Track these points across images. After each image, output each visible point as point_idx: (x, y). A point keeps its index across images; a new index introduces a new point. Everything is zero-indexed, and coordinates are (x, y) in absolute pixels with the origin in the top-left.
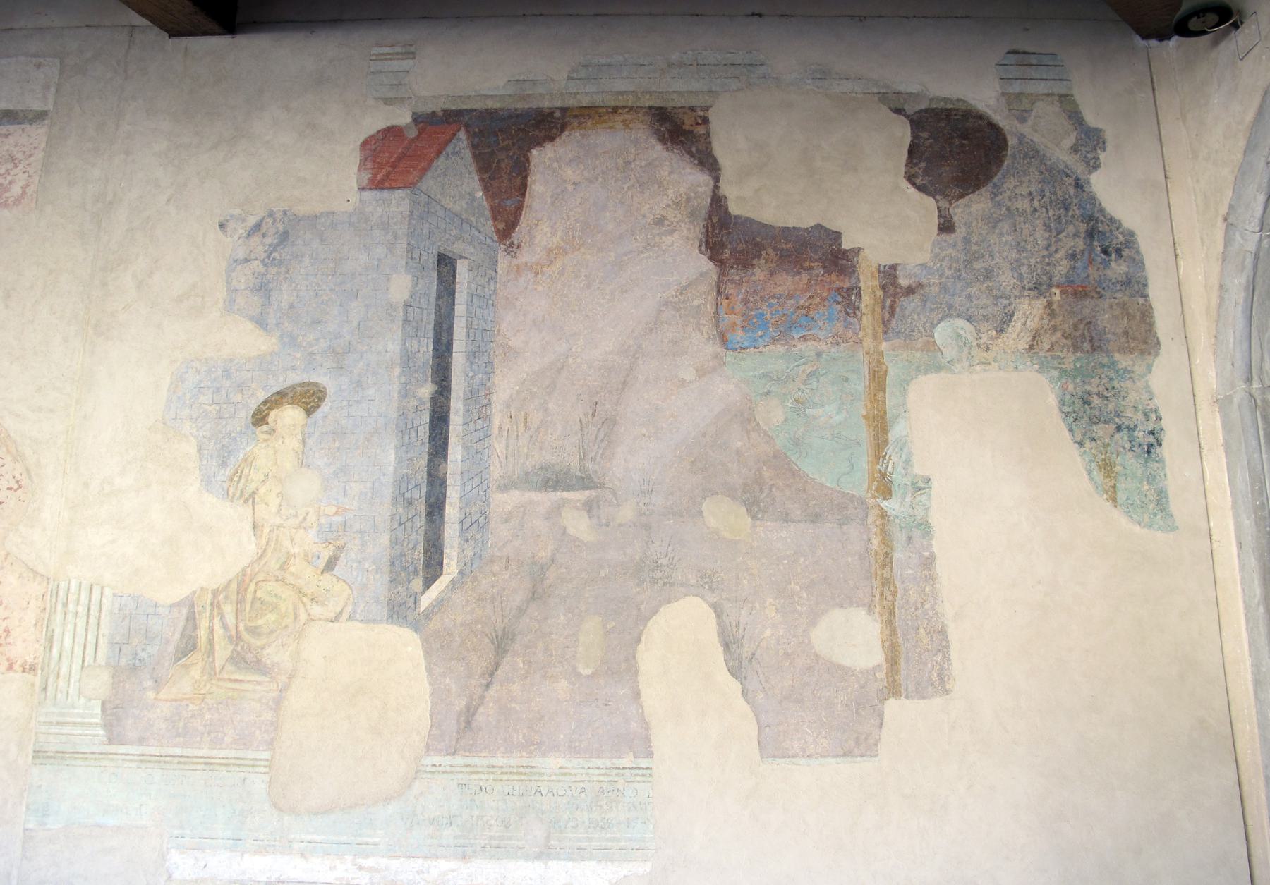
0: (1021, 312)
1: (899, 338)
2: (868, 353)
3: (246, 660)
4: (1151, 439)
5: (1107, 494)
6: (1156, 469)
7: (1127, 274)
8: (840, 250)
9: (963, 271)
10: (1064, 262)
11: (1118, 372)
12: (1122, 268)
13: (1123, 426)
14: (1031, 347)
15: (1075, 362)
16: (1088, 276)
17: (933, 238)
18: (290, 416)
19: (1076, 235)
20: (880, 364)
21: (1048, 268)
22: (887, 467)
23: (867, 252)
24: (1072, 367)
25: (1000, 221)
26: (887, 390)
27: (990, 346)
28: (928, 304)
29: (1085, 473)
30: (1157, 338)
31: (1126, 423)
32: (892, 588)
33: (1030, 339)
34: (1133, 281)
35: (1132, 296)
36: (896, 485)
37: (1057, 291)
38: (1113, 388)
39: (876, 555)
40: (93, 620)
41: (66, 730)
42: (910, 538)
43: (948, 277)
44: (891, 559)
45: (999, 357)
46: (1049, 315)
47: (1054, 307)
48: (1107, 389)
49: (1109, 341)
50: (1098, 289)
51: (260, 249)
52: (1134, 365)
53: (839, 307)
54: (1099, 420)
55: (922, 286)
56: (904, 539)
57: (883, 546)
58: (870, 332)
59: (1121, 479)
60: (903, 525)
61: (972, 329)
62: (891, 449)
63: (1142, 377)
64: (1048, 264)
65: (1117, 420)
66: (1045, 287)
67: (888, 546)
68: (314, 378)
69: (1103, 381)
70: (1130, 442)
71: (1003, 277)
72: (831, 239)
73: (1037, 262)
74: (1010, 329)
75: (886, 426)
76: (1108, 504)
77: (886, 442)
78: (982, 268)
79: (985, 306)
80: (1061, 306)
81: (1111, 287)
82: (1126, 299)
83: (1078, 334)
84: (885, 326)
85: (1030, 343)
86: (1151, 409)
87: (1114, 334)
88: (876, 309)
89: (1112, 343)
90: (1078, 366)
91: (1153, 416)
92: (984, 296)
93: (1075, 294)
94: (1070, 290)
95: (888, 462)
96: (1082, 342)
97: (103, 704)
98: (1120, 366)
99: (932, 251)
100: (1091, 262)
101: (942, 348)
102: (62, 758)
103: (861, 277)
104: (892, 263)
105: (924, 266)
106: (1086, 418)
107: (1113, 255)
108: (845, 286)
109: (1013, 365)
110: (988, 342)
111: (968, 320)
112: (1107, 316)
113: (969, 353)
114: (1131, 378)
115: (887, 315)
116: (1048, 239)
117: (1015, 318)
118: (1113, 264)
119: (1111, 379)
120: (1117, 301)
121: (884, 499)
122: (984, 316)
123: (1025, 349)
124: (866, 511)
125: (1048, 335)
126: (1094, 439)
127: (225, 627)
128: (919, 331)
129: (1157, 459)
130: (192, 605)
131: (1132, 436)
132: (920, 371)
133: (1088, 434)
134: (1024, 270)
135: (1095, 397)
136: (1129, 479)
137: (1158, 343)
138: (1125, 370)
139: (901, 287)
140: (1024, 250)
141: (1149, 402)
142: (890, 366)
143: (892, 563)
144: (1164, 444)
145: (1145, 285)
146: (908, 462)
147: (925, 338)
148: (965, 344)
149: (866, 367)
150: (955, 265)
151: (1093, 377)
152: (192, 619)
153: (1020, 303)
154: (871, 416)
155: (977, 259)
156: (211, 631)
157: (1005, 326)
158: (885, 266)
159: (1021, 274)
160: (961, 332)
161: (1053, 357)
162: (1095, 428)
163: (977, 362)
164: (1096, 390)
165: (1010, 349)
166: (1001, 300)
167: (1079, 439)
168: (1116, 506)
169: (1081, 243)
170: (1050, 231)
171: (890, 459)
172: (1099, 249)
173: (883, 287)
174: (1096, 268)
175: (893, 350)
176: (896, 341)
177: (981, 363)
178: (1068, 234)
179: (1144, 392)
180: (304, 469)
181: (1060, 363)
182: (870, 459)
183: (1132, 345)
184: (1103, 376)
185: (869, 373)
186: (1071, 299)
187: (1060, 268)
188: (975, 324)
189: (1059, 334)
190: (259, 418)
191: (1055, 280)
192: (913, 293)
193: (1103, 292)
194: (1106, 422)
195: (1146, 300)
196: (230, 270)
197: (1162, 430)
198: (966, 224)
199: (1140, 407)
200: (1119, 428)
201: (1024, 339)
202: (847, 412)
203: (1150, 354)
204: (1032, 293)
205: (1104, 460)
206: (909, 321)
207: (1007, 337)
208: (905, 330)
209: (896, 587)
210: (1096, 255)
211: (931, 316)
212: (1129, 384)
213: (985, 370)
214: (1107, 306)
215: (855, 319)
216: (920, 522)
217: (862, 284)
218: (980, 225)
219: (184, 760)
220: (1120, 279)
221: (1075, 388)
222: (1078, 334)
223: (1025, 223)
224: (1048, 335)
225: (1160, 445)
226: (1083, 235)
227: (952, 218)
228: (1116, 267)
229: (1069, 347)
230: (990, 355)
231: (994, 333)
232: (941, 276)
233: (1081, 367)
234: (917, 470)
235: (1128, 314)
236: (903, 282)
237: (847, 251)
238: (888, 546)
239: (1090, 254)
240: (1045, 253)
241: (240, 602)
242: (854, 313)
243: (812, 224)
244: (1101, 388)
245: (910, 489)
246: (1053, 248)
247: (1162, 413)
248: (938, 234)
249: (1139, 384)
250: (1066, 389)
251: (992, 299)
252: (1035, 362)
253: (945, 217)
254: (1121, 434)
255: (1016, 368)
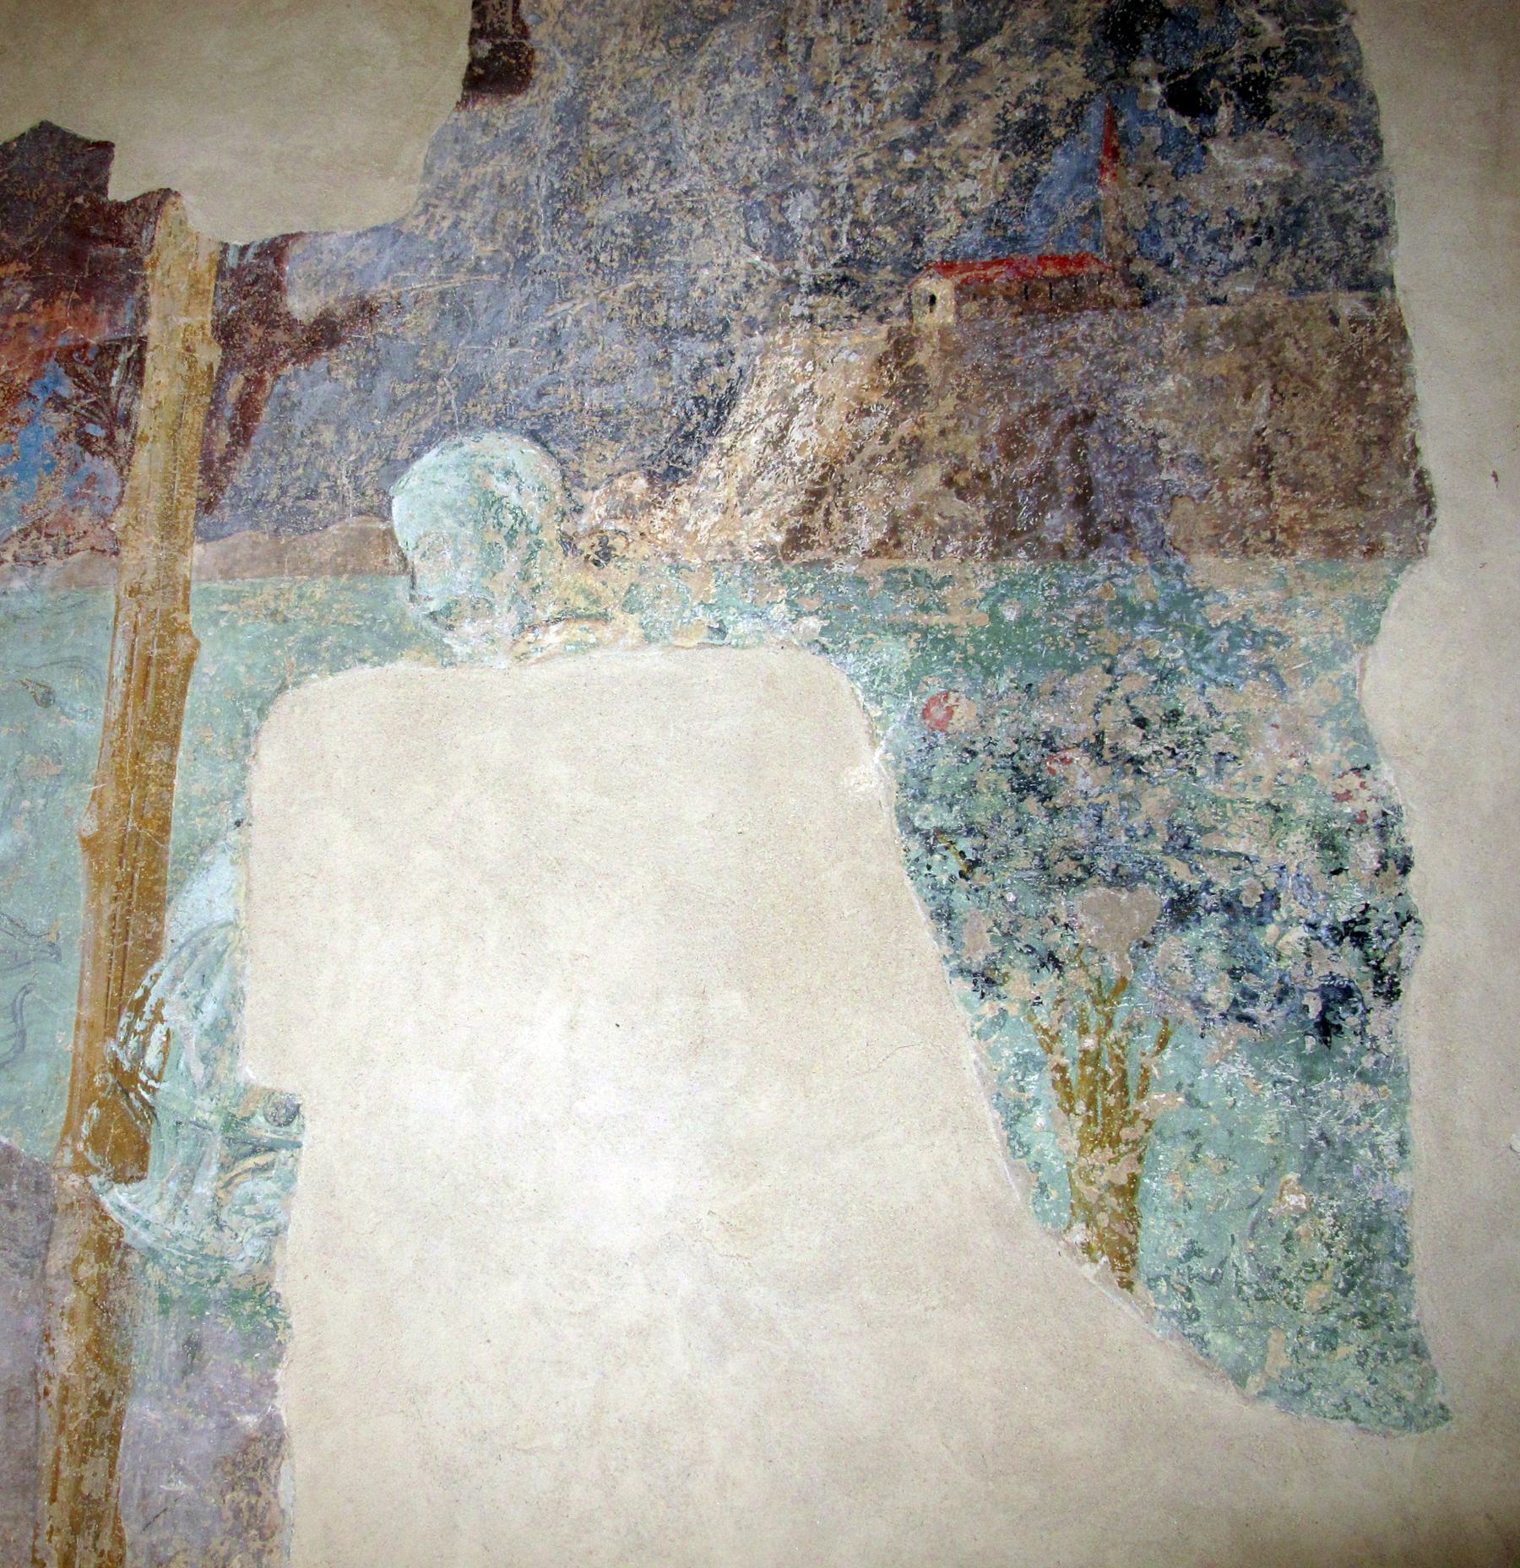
0: (767, 390)
1: (256, 526)
2: (134, 592)
4: (1347, 964)
5: (1090, 1222)
6: (1355, 1109)
7: (1285, 191)
8: (97, 208)
9: (541, 237)
10: (989, 160)
11: (1202, 640)
12: (1266, 162)
13: (1207, 900)
14: (798, 539)
15: (996, 599)
16: (1095, 212)
17: (441, 121)
19: (1052, 42)
20: (172, 629)
21: (909, 192)
22: (144, 1046)
23: (188, 199)
24: (979, 616)
25: (721, 18)
26: (185, 734)
27: (619, 542)
28: (385, 383)
29: (991, 1117)
30: (1420, 476)
31: (1225, 884)
32: (106, 1544)
33: (793, 502)
34: (1318, 215)
35: (1302, 286)
36: (166, 1121)
37: (943, 288)
38: (1174, 716)
39: (64, 1400)
42: (193, 1347)
43: (476, 269)
44: (117, 1424)
45: (647, 591)
46: (892, 392)
47: (922, 357)
48: (1141, 723)
49: (1171, 497)
50: (1137, 268)
52: (1286, 606)
53: (59, 421)
54: (1089, 870)
55: (372, 311)
56: (173, 1348)
57: (93, 1368)
58: (152, 507)
59: (1168, 1154)
60: (176, 1292)
61: (550, 473)
62: (167, 975)
63: (1326, 663)
64: (913, 176)
65: (1177, 869)
66: (886, 274)
67: (109, 1367)
69: (1126, 687)
70: (1234, 974)
71: (707, 245)
72: (72, 173)
73: (861, 172)
74: (710, 467)
75: (161, 881)
76: (1089, 1270)
77: (152, 946)
78: (621, 216)
79: (618, 373)
80: (952, 352)
81: (1203, 250)
82: (1273, 301)
83: (1019, 472)
84: (212, 482)
85: (793, 522)
86: (1360, 819)
87: (1197, 463)
88: (189, 417)
89: (1184, 506)
90: (1010, 615)
91: (1365, 852)
92: (617, 330)
93: (1026, 296)
94: (1001, 277)
95: (149, 1030)
96: (1041, 508)
98: (1215, 613)
99: (429, 171)
100: (1114, 148)
101: (414, 558)
103: (153, 300)
104: (272, 232)
105: (390, 233)
106: (1023, 860)
107: (1224, 113)
108: (93, 342)
109: (708, 618)
110: (609, 527)
111: (534, 436)
112: (1169, 384)
113: (525, 577)
114: (1268, 668)
115: (225, 436)
116: (917, 71)
117: (738, 416)
118: (1220, 152)
119: (1167, 676)
120: (1226, 313)
121: (120, 1178)
122: (604, 415)
123: (768, 549)
124: (46, 1218)
125: (880, 483)
126: (1052, 960)
128: (335, 495)
129: (1368, 1062)
131: (1253, 947)
132: (314, 656)
133: (1028, 935)
134: (801, 208)
135: (1080, 760)
136: (1209, 1154)
137: (1425, 498)
138: (1241, 631)
139: (291, 325)
140: (811, 124)
141: (1353, 781)
142: (207, 636)
143: (115, 1439)
144: (1413, 989)
145: (1377, 234)
146: (222, 1033)
147: (353, 522)
148: (512, 535)
149: (121, 646)
150: (510, 216)
151: (1075, 668)
153: (765, 352)
154: (113, 837)
155: (601, 183)
157: (690, 454)
158: (243, 250)
159: (786, 227)
160: (502, 487)
161: (893, 582)
162: (1061, 904)
163: (552, 610)
164: (1086, 728)
165: (701, 550)
166: (682, 344)
167: (978, 959)
168: (1128, 1285)
169: (1077, 72)
170: (934, 36)
171: (158, 1017)
172: (1157, 89)
173: (226, 332)
174: (1133, 175)
175: (227, 574)
176: (243, 539)
177: (568, 616)
178: (1016, 41)
179: (1326, 735)
181: (924, 608)
182: (86, 1013)
183: (1288, 512)
184: (1127, 660)
185: (129, 669)
186: (1005, 316)
187: (966, 189)
188: (566, 452)
189: (931, 476)
191: (936, 242)
192: (333, 341)
193: (1158, 278)
194: (1120, 879)
195: (1372, 303)
197: (1406, 919)
198: (576, 51)
199: (1303, 807)
200: (1182, 909)
201: (770, 505)
202: (34, 822)
203: (1373, 550)
204: (827, 305)
205: (1090, 1059)
206: (301, 454)
207: (695, 501)
208: (283, 491)
209: (120, 1541)
210: (1145, 118)
211: (390, 431)
212: (1253, 696)
213: (582, 648)
214: (1173, 338)
215: (108, 463)
216: (243, 1285)
217: (152, 328)
218: (634, 45)
220: (1250, 213)
221: (983, 721)
222: (1019, 472)
223: (825, 16)
224: (880, 483)
225: (1392, 994)
226: (1084, 38)
227: (525, 33)
228: (1240, 164)
229: (972, 532)
230: (618, 575)
231: (642, 483)
232: (452, 264)
233: (1024, 620)
234: (252, 1070)
235: (1278, 369)
236: (301, 304)
237: (121, 207)
238: (109, 1367)
239: (1111, 123)
240: (905, 129)
242: (110, 438)
243: (24, 124)
244: (1114, 717)
245: (217, 1148)
246: (942, 106)
247: (1415, 834)
248: (463, 103)
249: (1304, 696)
250: (941, 725)
251: (647, 341)
252: (815, 604)
253: (501, 33)
254: (1194, 935)
255: (721, 631)
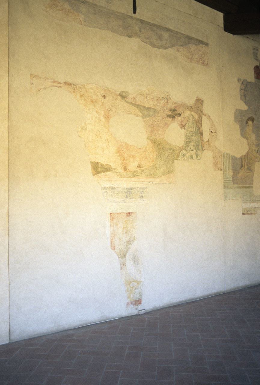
3: (249, 169)
18: (250, 123)
40: (229, 161)
41: (227, 182)
51: (244, 87)
68: (253, 116)
97: (232, 177)
102: (228, 187)
127: (246, 162)
130: (242, 158)
152: (242, 161)
156: (244, 162)
180: (253, 134)
190: (247, 123)
196: (240, 91)
219: (243, 187)
241: (247, 158)
